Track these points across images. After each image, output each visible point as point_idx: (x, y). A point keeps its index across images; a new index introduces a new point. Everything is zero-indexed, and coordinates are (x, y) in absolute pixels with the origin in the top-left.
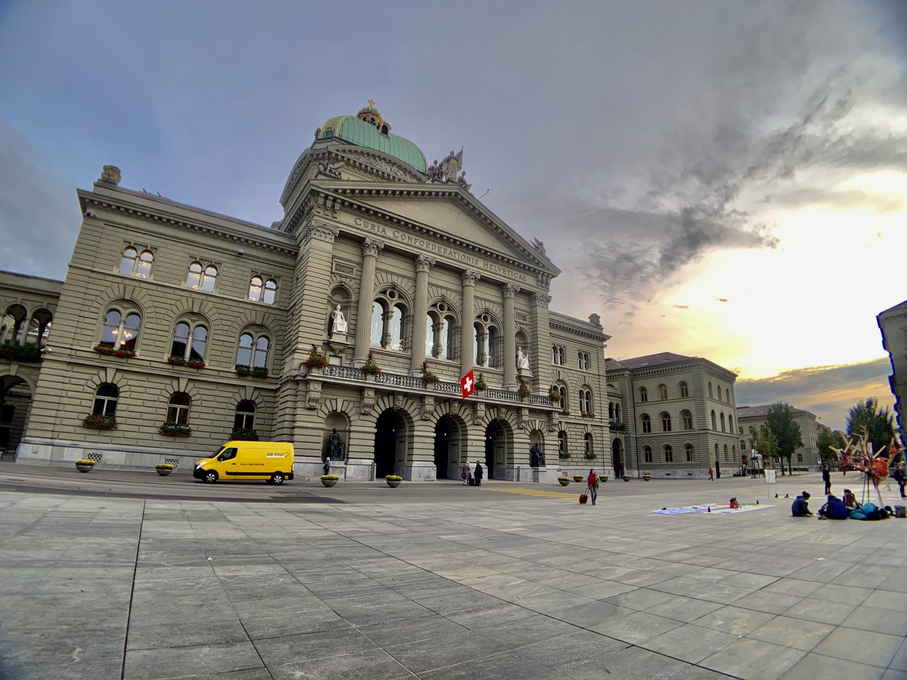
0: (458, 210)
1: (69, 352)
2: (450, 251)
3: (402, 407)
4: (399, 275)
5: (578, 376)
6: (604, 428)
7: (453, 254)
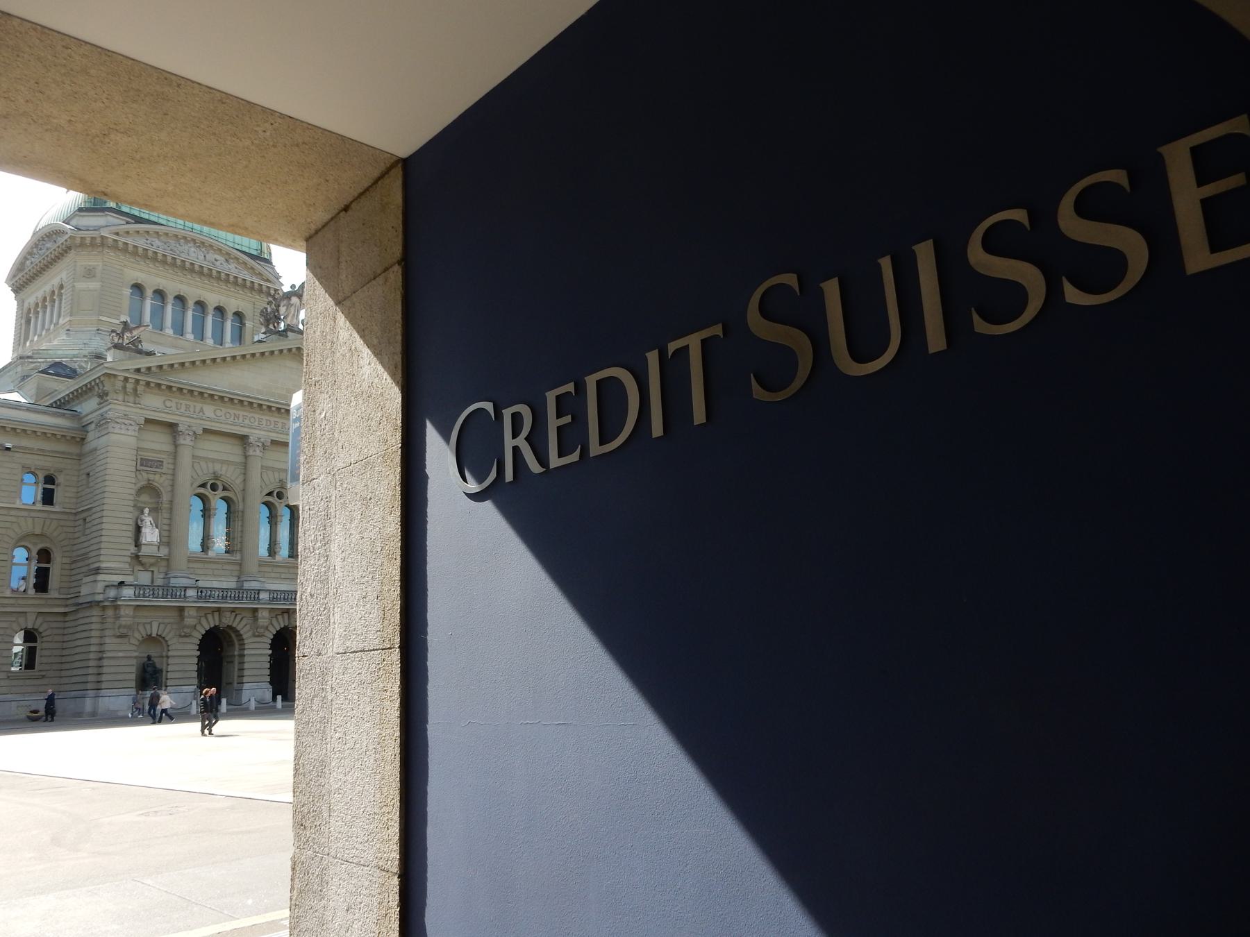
3: (230, 624)
4: (222, 462)
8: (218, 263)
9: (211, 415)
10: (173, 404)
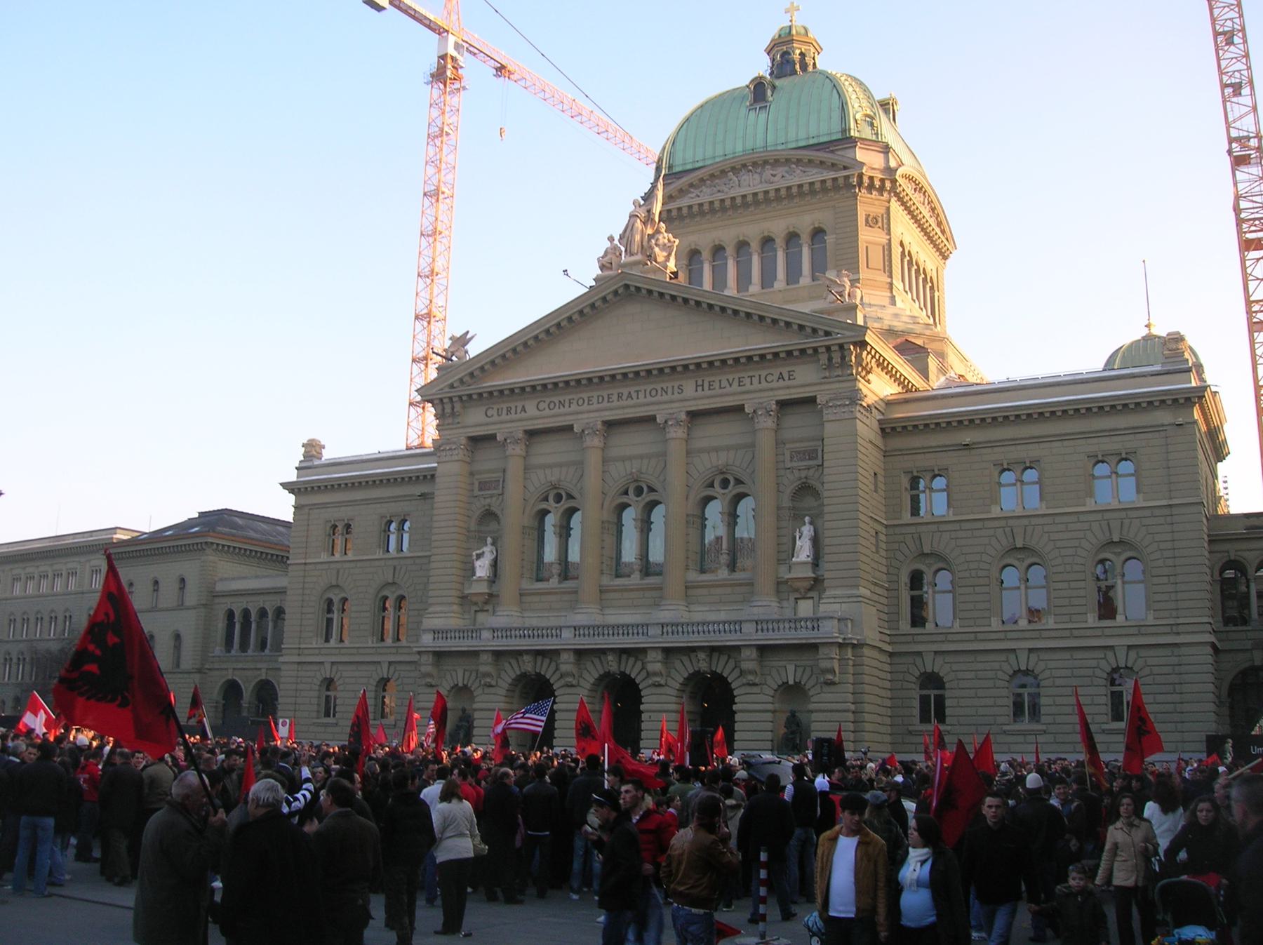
1: (296, 651)
2: (630, 393)
4: (560, 465)
5: (1086, 526)
6: (1184, 650)
7: (634, 395)
8: (776, 179)
9: (536, 413)
10: (495, 414)
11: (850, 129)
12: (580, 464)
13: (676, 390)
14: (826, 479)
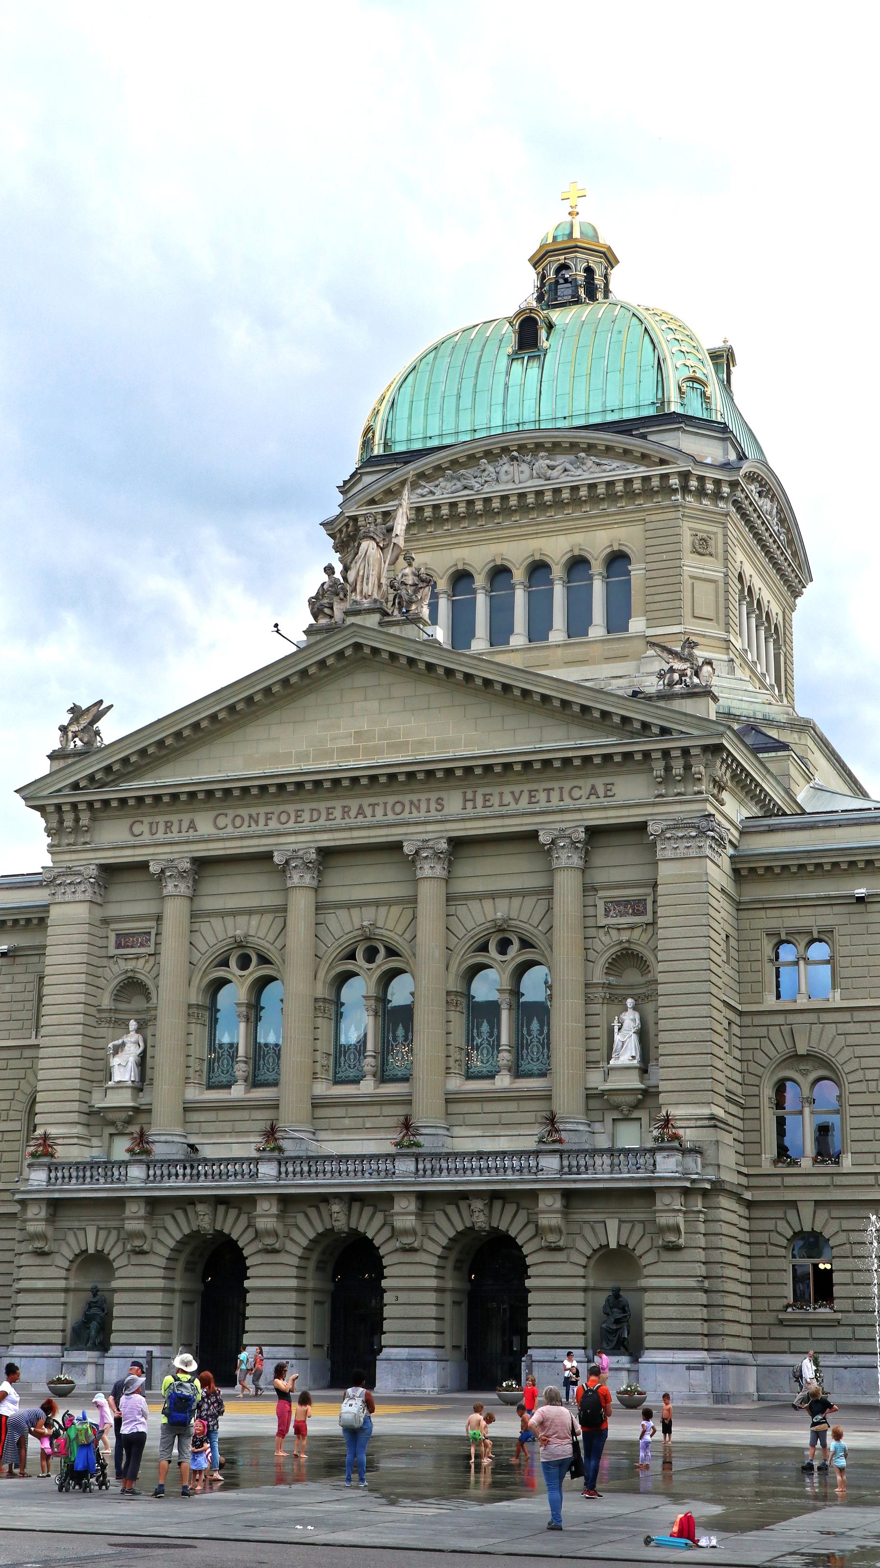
0: (386, 678)
2: (361, 807)
7: (368, 811)
8: (554, 473)
11: (669, 402)
12: (282, 910)
13: (433, 806)
14: (661, 944)
